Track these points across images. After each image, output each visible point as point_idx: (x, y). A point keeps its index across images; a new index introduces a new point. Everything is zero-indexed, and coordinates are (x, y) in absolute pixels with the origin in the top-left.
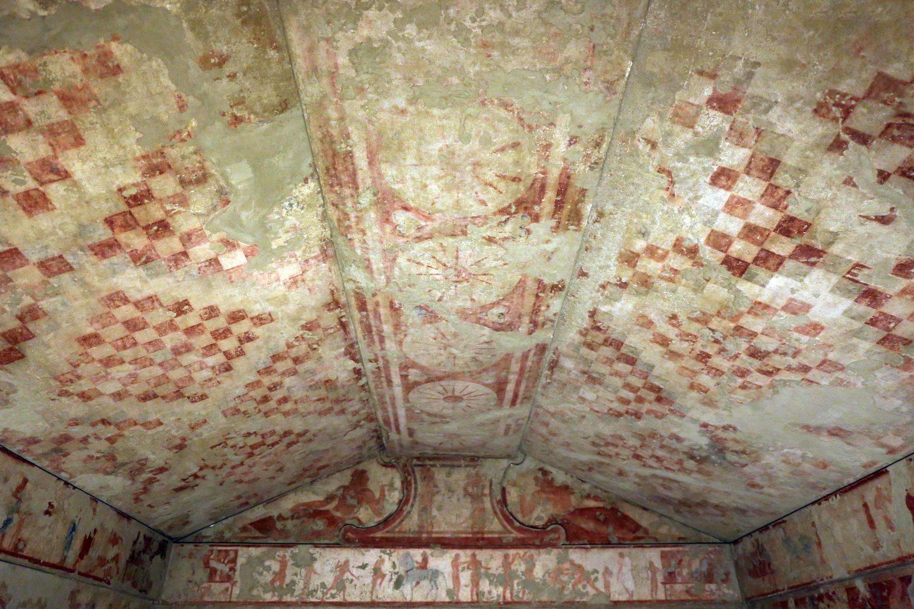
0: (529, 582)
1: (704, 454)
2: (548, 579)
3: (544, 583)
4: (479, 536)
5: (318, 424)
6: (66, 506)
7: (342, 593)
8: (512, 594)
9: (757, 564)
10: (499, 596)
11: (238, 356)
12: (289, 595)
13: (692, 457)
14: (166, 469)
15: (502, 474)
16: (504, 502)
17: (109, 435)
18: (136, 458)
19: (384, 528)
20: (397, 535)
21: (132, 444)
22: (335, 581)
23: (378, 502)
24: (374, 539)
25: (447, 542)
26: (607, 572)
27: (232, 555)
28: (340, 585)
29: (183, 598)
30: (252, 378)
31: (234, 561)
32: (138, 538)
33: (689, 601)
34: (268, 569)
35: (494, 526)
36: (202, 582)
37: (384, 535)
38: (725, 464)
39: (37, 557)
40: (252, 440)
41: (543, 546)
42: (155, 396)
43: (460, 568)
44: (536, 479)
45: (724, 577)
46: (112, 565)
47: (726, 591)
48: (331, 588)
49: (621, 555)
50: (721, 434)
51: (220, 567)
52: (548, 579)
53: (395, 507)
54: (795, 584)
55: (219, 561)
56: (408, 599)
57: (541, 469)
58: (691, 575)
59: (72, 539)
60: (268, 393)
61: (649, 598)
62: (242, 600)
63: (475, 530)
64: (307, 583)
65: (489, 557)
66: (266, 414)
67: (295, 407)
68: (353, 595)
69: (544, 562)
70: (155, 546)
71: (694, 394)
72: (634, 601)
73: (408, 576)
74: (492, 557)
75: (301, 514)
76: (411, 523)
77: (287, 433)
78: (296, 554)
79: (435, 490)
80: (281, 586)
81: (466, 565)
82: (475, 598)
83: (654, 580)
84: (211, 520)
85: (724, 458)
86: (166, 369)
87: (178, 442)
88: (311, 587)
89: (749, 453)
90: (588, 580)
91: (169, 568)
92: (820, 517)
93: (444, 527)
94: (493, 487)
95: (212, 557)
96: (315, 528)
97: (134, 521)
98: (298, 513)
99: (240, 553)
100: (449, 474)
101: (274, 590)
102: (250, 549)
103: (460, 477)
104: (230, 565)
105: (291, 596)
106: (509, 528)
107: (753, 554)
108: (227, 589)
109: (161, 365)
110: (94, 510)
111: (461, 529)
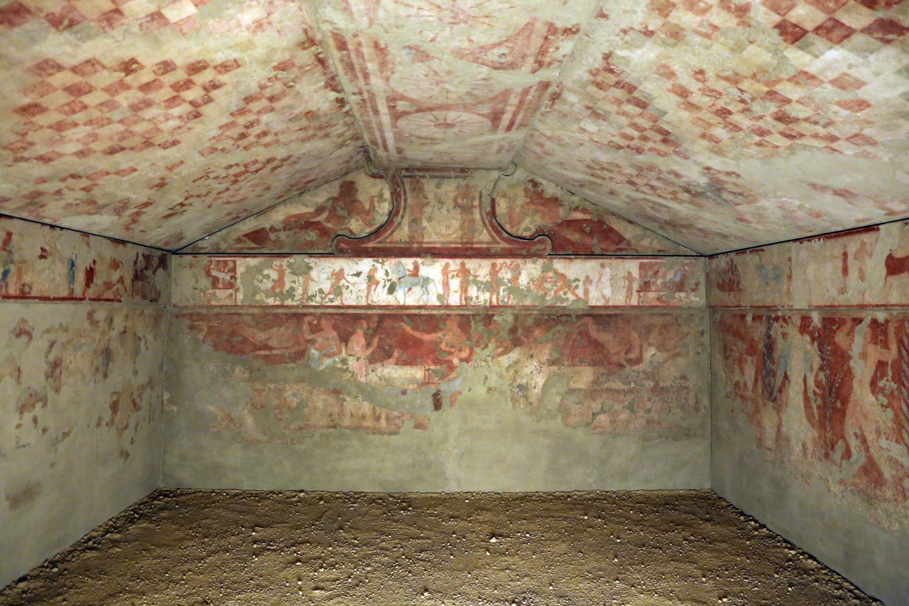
0: (514, 289)
1: (700, 190)
2: (532, 287)
3: (529, 290)
4: (469, 246)
5: (298, 150)
6: (59, 247)
8: (498, 299)
9: (727, 281)
10: (486, 301)
11: (205, 103)
12: (290, 300)
13: (688, 191)
14: (151, 204)
16: (493, 214)
17: (83, 186)
18: (118, 199)
19: (375, 239)
20: (389, 245)
21: (110, 189)
23: (368, 213)
24: (366, 248)
25: (437, 252)
26: (588, 280)
27: (231, 265)
28: (337, 291)
29: (192, 302)
30: (225, 120)
31: (233, 270)
32: (137, 258)
33: (659, 307)
34: (268, 277)
35: (484, 237)
36: (208, 289)
38: (719, 200)
39: (46, 295)
40: (235, 170)
42: (122, 149)
43: (450, 276)
45: (694, 286)
46: (119, 286)
47: (693, 298)
48: (329, 294)
49: (603, 266)
50: (722, 177)
51: (221, 275)
52: (532, 287)
53: (385, 218)
54: (757, 305)
55: (219, 270)
56: (402, 303)
58: (664, 284)
59: (74, 273)
60: (245, 130)
61: (623, 304)
64: (305, 290)
65: (477, 266)
66: (246, 148)
67: (276, 138)
68: (350, 299)
69: (529, 271)
70: (155, 261)
71: (705, 143)
72: (609, 307)
74: (480, 266)
76: (402, 234)
77: (269, 161)
79: (425, 201)
80: (281, 292)
81: (455, 273)
82: (464, 302)
83: (630, 289)
85: (720, 196)
86: (128, 125)
87: (157, 182)
88: (310, 293)
89: (745, 195)
90: (569, 287)
92: (798, 254)
93: (434, 238)
94: (483, 199)
96: (308, 238)
97: (129, 245)
98: (290, 224)
99: (238, 263)
101: (275, 295)
104: (230, 274)
105: (292, 300)
106: (497, 238)
107: (725, 272)
108: (231, 295)
109: (121, 122)
110: (88, 244)
111: (451, 240)
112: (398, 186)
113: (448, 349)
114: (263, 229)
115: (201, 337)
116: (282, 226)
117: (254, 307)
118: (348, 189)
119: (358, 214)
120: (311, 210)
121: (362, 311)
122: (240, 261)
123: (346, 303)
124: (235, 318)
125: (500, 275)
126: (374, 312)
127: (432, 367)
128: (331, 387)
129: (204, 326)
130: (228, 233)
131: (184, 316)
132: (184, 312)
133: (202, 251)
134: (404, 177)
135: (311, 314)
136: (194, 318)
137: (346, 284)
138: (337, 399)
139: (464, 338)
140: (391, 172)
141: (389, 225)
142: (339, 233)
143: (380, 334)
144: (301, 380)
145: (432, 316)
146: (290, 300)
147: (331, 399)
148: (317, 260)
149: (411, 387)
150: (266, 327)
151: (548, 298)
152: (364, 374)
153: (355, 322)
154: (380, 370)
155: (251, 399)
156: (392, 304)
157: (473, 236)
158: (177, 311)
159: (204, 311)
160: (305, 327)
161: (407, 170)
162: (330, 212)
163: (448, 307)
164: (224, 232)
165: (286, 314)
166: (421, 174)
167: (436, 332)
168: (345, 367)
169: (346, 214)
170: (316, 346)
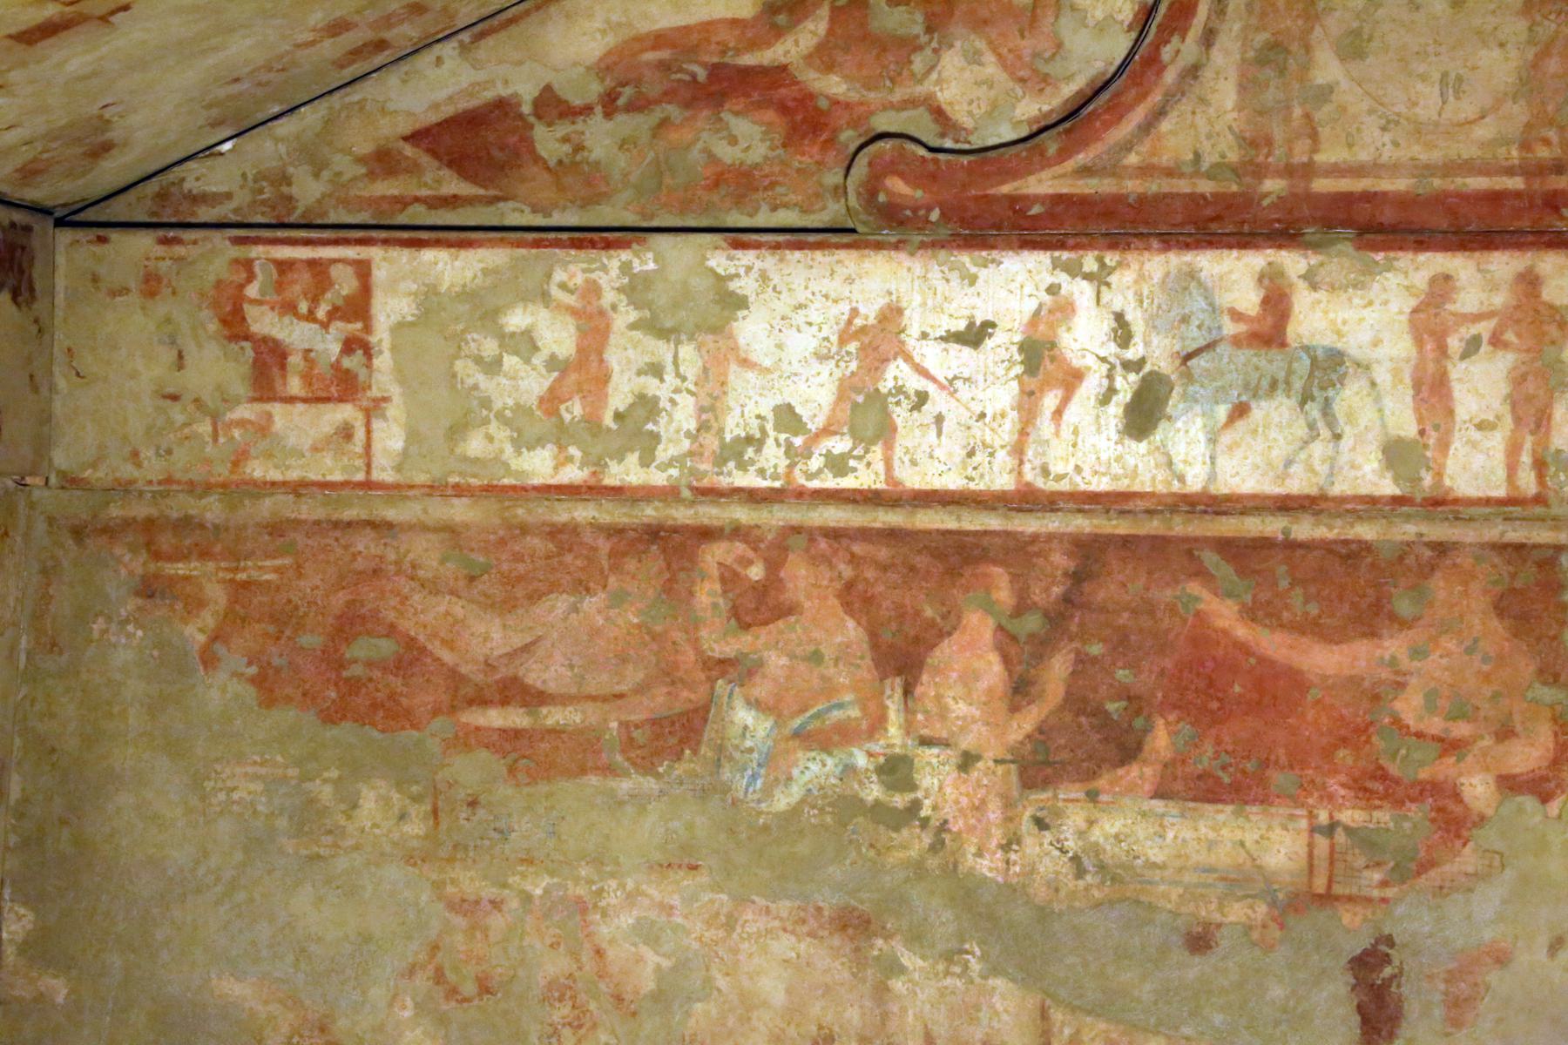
7: (877, 452)
12: (633, 459)
19: (1064, 154)
22: (841, 396)
24: (1016, 203)
25: (1388, 216)
27: (345, 283)
28: (866, 412)
29: (153, 467)
31: (358, 308)
34: (526, 343)
36: (230, 402)
37: (1064, 189)
43: (1454, 344)
48: (827, 431)
51: (295, 334)
53: (1119, 46)
55: (289, 308)
56: (1195, 480)
62: (422, 478)
63: (1543, 153)
68: (931, 458)
75: (653, 89)
76: (1199, 128)
78: (646, 280)
80: (592, 423)
81: (1484, 329)
82: (1528, 482)
84: (216, 124)
88: (733, 427)
91: (61, 339)
93: (1373, 144)
95: (252, 291)
96: (727, 154)
99: (380, 274)
101: (561, 436)
102: (428, 255)
104: (340, 329)
105: (646, 462)
108: (346, 433)
111: (1469, 151)
113: (1435, 725)
114: (503, 106)
115: (195, 633)
116: (595, 89)
117: (460, 491)
119: (980, 24)
121: (993, 522)
122: (388, 263)
123: (913, 480)
124: (364, 543)
126: (1052, 524)
127: (1351, 816)
128: (829, 901)
129: (210, 580)
130: (328, 122)
131: (110, 531)
132: (115, 512)
133: (205, 214)
135: (737, 532)
136: (166, 541)
137: (914, 383)
138: (859, 960)
139: (1526, 668)
141: (1137, 80)
142: (882, 123)
143: (1084, 636)
144: (681, 860)
145: (1352, 553)
146: (633, 459)
147: (828, 960)
148: (765, 261)
149: (1237, 913)
150: (515, 592)
152: (997, 836)
153: (953, 573)
154: (1075, 818)
155: (435, 948)
156: (1143, 484)
158: (77, 506)
159: (212, 510)
160: (707, 595)
163: (1440, 504)
164: (311, 117)
165: (614, 532)
167: (1373, 634)
168: (899, 800)
169: (918, 29)
170: (761, 690)
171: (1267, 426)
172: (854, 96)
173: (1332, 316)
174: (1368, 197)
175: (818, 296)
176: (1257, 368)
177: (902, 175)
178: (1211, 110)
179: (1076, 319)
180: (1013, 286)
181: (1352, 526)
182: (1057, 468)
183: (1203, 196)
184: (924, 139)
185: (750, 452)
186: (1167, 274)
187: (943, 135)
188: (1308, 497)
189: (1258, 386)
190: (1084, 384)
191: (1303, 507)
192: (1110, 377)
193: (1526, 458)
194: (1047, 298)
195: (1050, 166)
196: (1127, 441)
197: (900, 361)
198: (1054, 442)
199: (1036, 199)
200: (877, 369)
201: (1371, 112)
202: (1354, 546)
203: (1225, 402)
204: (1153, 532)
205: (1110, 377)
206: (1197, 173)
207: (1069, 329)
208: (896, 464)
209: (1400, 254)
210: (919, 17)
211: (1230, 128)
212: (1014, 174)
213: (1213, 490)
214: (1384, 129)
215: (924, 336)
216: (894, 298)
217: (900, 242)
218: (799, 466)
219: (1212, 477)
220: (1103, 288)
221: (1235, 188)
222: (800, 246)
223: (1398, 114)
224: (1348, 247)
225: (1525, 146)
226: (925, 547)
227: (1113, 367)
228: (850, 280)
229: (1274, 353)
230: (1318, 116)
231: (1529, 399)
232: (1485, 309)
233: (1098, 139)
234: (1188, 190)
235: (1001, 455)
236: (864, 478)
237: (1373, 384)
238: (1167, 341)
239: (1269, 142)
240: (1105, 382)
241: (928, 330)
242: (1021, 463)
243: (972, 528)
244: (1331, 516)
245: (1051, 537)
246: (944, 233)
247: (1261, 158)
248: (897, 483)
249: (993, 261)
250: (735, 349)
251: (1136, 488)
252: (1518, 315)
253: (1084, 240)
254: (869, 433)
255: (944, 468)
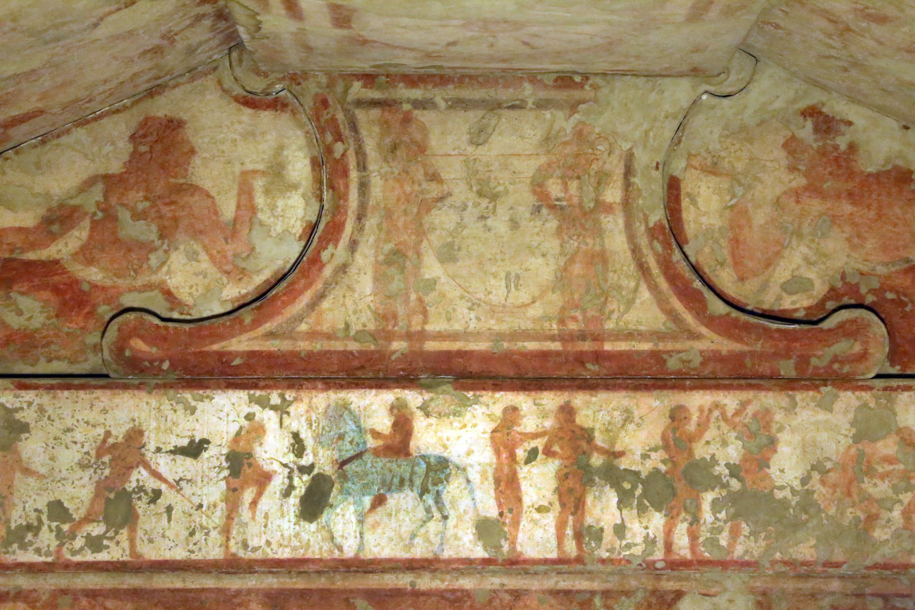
0: (751, 501)
3: (807, 503)
4: (587, 346)
8: (693, 537)
10: (650, 542)
15: (668, 133)
16: (673, 231)
19: (256, 323)
20: (303, 346)
22: (97, 495)
23: (232, 231)
25: (475, 367)
28: (118, 505)
35: (639, 314)
41: (806, 380)
43: (521, 453)
44: (791, 146)
52: (820, 491)
53: (293, 250)
56: (350, 550)
57: (811, 112)
63: (572, 326)
65: (618, 416)
68: (163, 538)
73: (344, 477)
74: (628, 417)
76: (348, 306)
79: (434, 190)
81: (539, 443)
93: (464, 319)
94: (636, 180)
96: (14, 321)
100: (479, 137)
103: (518, 144)
106: (689, 318)
112: (339, 137)
118: (162, 146)
119: (196, 234)
120: (28, 219)
121: (209, 582)
123: (150, 553)
125: (700, 451)
134: (359, 103)
137: (152, 484)
140: (312, 88)
141: (305, 274)
142: (129, 300)
148: (45, 399)
151: (879, 534)
157: (603, 314)
161: (369, 79)
162: (95, 225)
163: (515, 564)
166: (417, 93)
171: (398, 511)
172: (108, 283)
173: (440, 434)
174: (461, 354)
175: (82, 423)
176: (391, 471)
177: (142, 338)
178: (356, 295)
179: (266, 438)
180: (222, 415)
181: (457, 580)
182: (253, 542)
183: (351, 353)
184: (158, 312)
185: (29, 537)
186: (329, 406)
187: (172, 310)
188: (427, 560)
189: (391, 483)
190: (272, 483)
191: (423, 568)
192: (290, 478)
193: (569, 532)
194: (245, 423)
195: (247, 331)
196: (302, 523)
197: (141, 469)
198: (251, 524)
199: (236, 354)
200: (124, 474)
201: (462, 297)
202: (459, 594)
203: (369, 494)
204: (321, 587)
205: (290, 478)
206: (347, 337)
207: (261, 444)
208: (138, 542)
209: (484, 392)
210: (154, 228)
211: (369, 306)
212: (222, 338)
213: (362, 556)
214: (470, 309)
215: (159, 450)
216: (137, 423)
217: (141, 384)
218: (67, 545)
219: (361, 546)
220: (285, 416)
221: (373, 347)
222: (68, 387)
223: (479, 299)
224: (449, 388)
225: (562, 322)
226: (159, 601)
227: (292, 471)
228: (104, 411)
229: (402, 461)
230: (427, 299)
231: (571, 491)
232: (540, 430)
233: (280, 313)
234: (341, 349)
235: (214, 534)
236: (114, 553)
237: (468, 481)
238: (329, 452)
239: (395, 316)
240: (287, 481)
241: (161, 446)
242: (228, 539)
243: (193, 586)
244: (442, 572)
245: (249, 591)
246: (173, 377)
247: (390, 327)
248: (140, 556)
249: (207, 397)
250: (19, 461)
251: (309, 555)
252: (560, 434)
253: (271, 383)
254: (119, 519)
255: (173, 544)
